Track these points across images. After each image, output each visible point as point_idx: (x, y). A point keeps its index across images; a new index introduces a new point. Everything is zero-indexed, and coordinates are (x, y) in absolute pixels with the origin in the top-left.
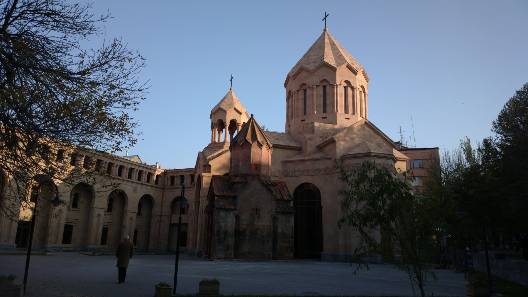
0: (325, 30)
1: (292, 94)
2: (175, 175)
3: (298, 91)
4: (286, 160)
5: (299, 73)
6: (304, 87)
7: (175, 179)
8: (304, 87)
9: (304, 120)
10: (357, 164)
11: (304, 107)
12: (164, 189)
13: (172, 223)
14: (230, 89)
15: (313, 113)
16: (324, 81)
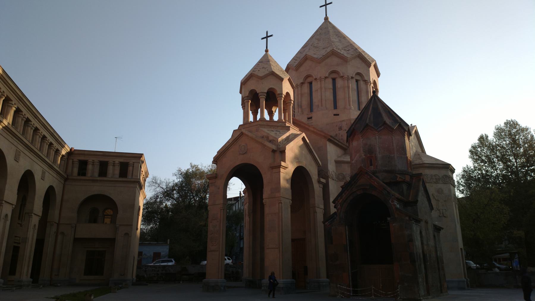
0: (326, 19)
1: (309, 80)
2: (90, 159)
3: (326, 78)
4: (339, 159)
5: (328, 57)
6: (334, 76)
7: (90, 167)
8: (334, 76)
9: (338, 115)
10: (435, 175)
11: (332, 99)
12: (66, 180)
13: (76, 237)
14: (267, 51)
15: (350, 109)
16: (358, 74)
